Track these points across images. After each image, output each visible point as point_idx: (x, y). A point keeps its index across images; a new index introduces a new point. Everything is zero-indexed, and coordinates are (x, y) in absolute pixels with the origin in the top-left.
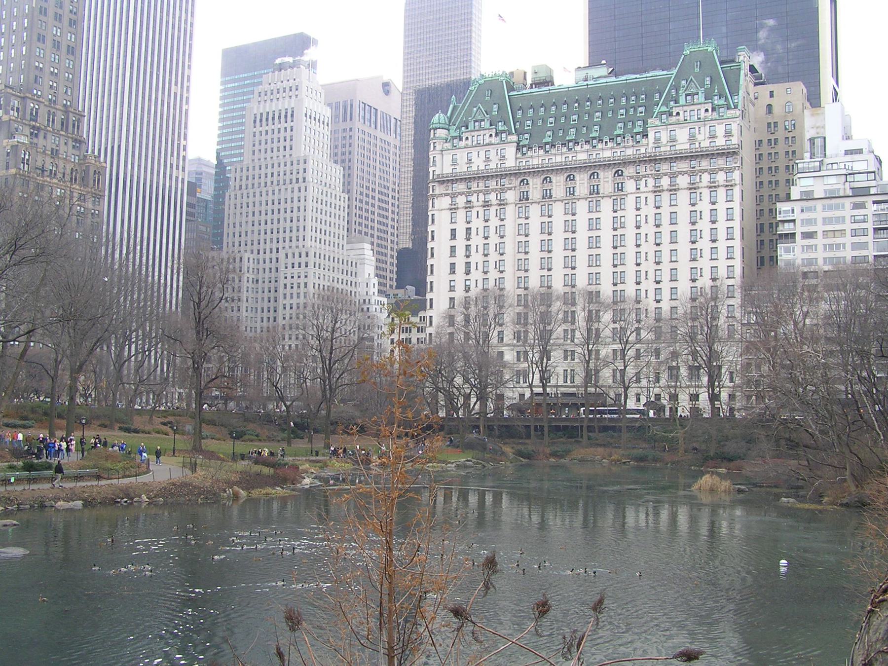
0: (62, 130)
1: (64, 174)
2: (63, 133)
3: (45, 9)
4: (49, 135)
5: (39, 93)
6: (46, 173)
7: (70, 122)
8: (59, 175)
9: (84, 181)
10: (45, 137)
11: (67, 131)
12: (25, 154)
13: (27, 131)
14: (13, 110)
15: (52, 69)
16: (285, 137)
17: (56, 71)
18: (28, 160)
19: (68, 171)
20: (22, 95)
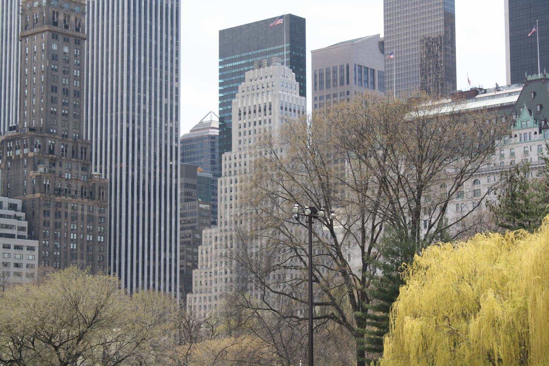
0: (73, 157)
1: (76, 191)
2: (74, 160)
3: (56, 87)
4: (63, 164)
5: (55, 131)
6: (62, 193)
7: (81, 153)
8: (73, 193)
9: (91, 197)
10: (60, 165)
11: (77, 158)
12: (46, 181)
13: (47, 162)
14: (36, 147)
15: (63, 111)
16: (230, 164)
17: (66, 112)
18: (49, 186)
19: (79, 189)
20: (42, 135)
